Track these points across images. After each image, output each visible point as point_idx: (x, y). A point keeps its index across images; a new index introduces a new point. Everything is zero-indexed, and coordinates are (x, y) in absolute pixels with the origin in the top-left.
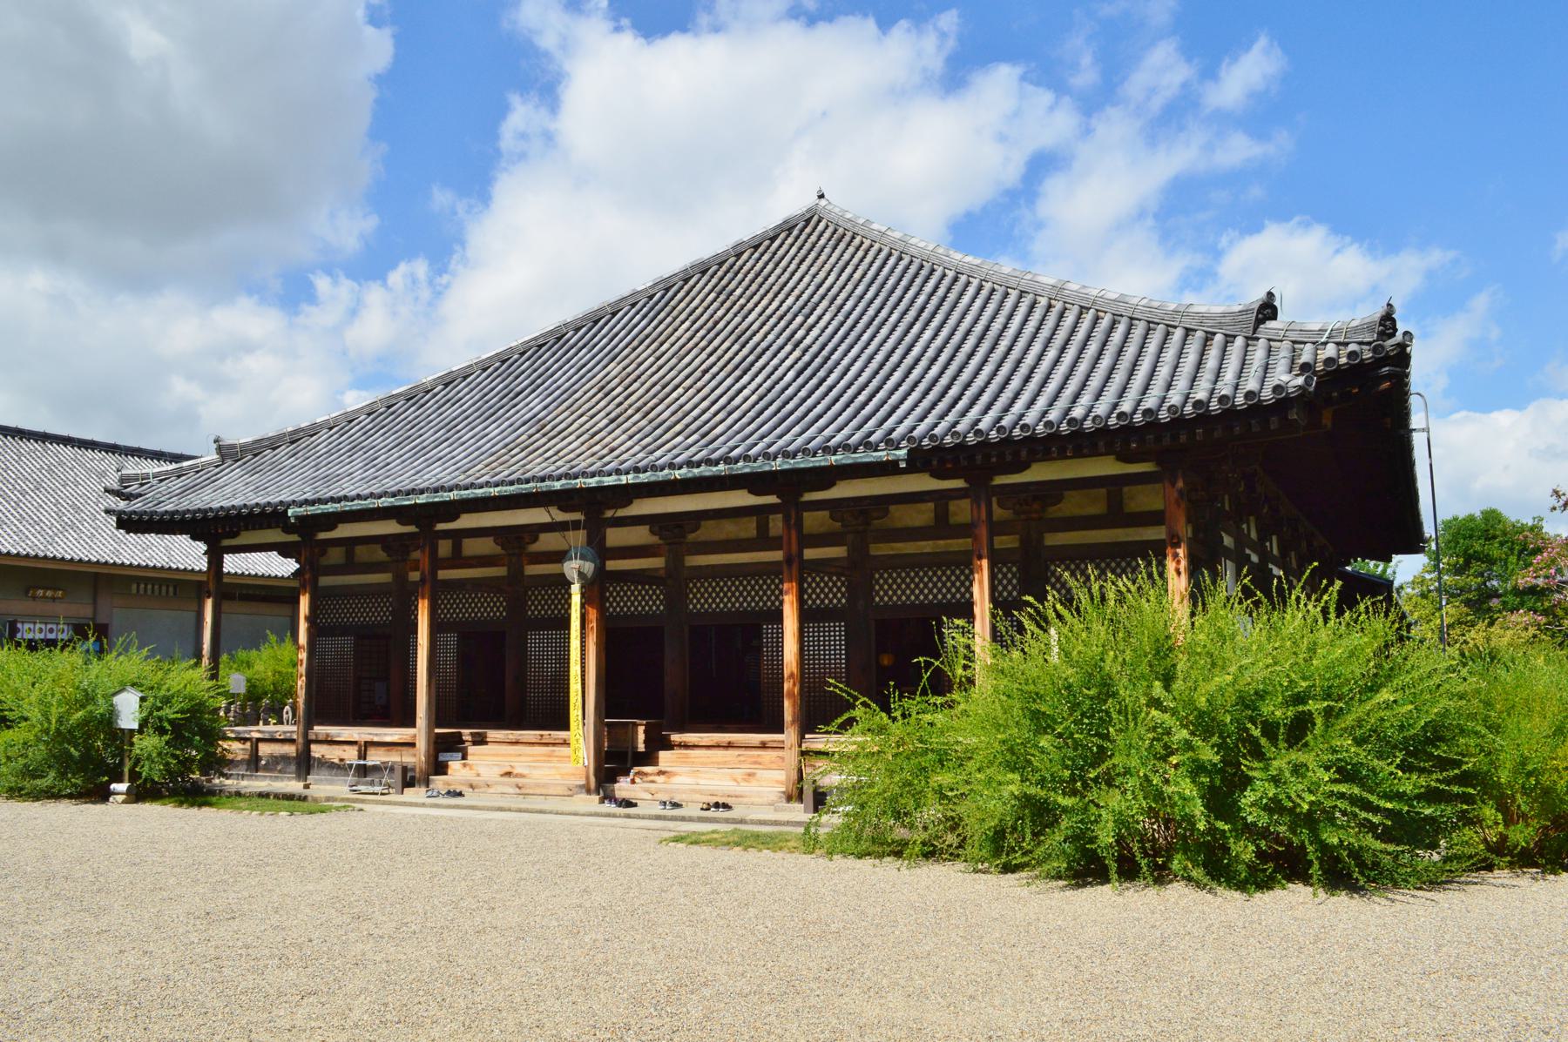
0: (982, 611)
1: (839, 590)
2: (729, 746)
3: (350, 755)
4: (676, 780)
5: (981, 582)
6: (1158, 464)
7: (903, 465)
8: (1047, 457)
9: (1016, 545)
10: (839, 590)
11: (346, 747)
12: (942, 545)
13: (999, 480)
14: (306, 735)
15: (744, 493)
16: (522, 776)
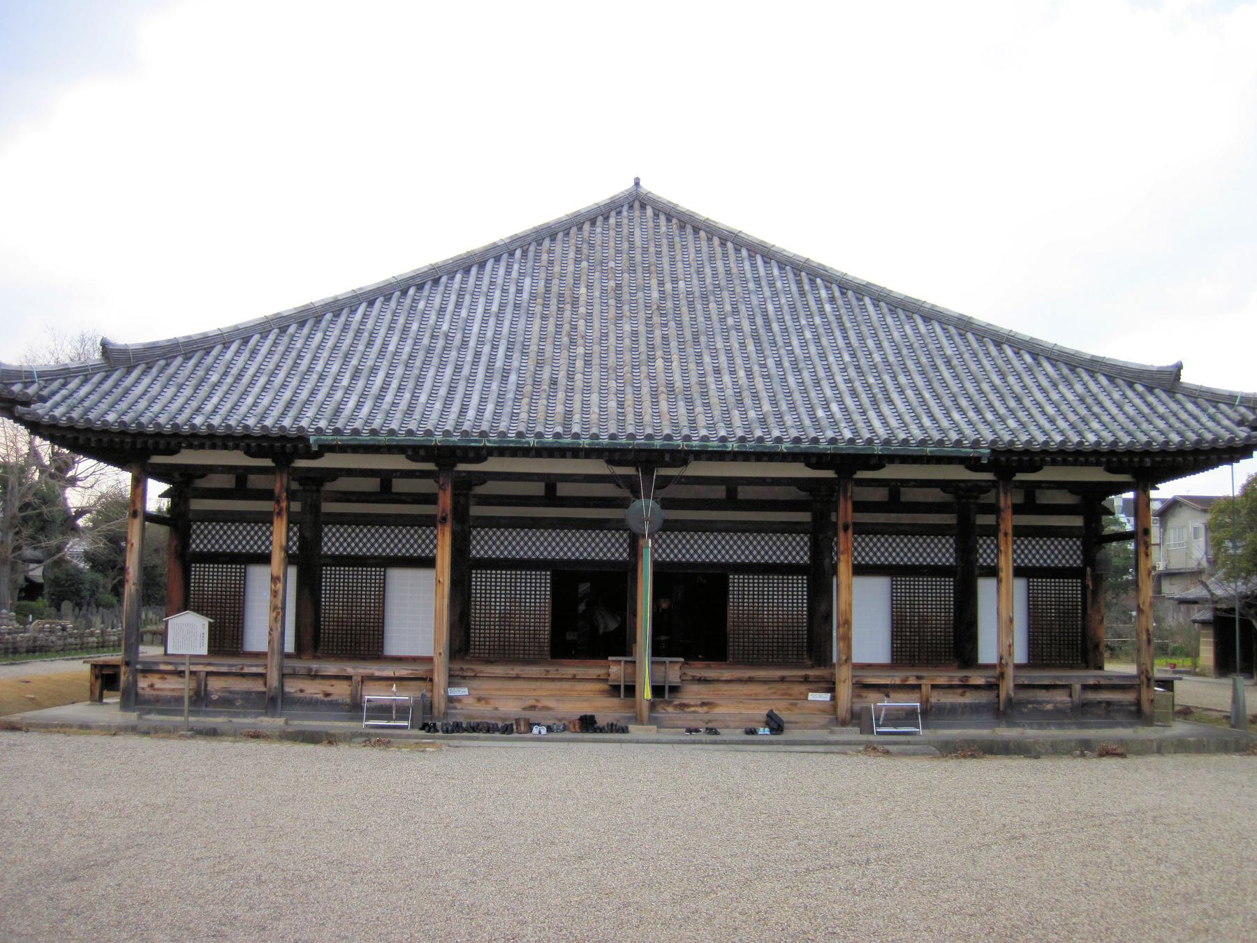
0: (1007, 576)
1: (802, 549)
2: (750, 680)
3: (341, 691)
4: (717, 711)
5: (1006, 553)
6: (1135, 476)
7: (985, 461)
8: (1054, 463)
9: (954, 522)
10: (802, 549)
11: (333, 682)
12: (893, 518)
13: (1020, 477)
14: (281, 667)
15: (802, 465)
16: (548, 708)
